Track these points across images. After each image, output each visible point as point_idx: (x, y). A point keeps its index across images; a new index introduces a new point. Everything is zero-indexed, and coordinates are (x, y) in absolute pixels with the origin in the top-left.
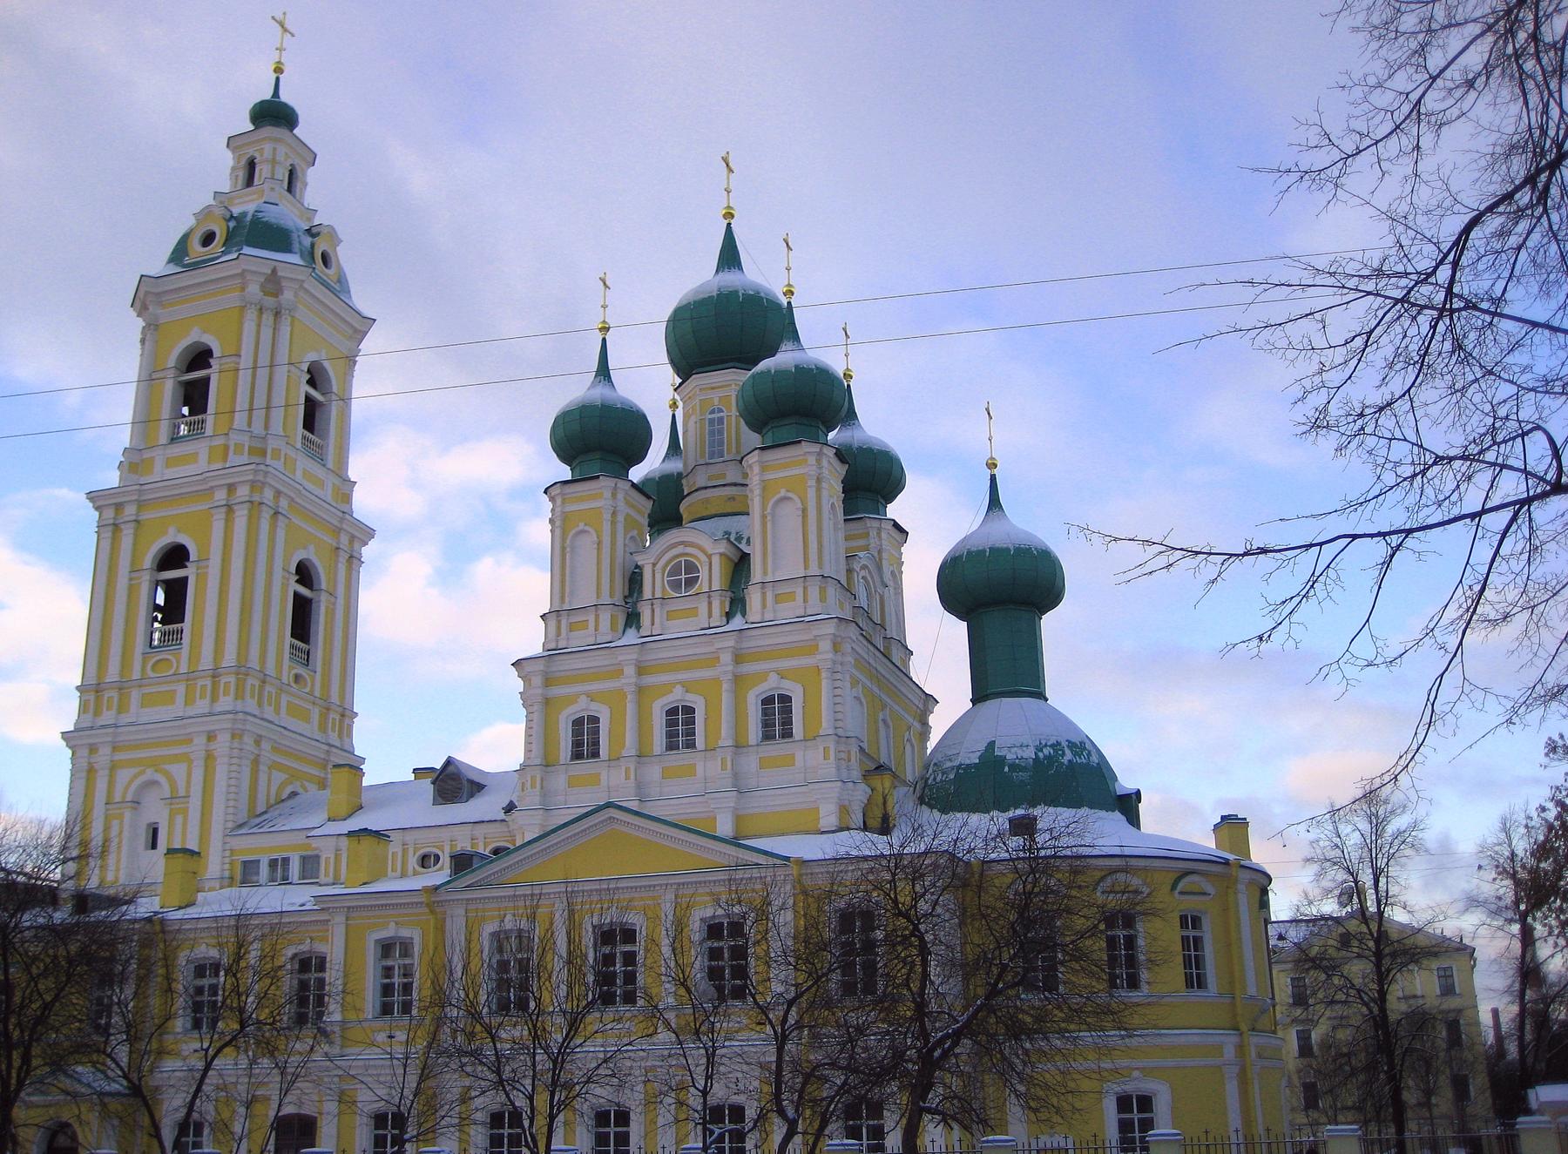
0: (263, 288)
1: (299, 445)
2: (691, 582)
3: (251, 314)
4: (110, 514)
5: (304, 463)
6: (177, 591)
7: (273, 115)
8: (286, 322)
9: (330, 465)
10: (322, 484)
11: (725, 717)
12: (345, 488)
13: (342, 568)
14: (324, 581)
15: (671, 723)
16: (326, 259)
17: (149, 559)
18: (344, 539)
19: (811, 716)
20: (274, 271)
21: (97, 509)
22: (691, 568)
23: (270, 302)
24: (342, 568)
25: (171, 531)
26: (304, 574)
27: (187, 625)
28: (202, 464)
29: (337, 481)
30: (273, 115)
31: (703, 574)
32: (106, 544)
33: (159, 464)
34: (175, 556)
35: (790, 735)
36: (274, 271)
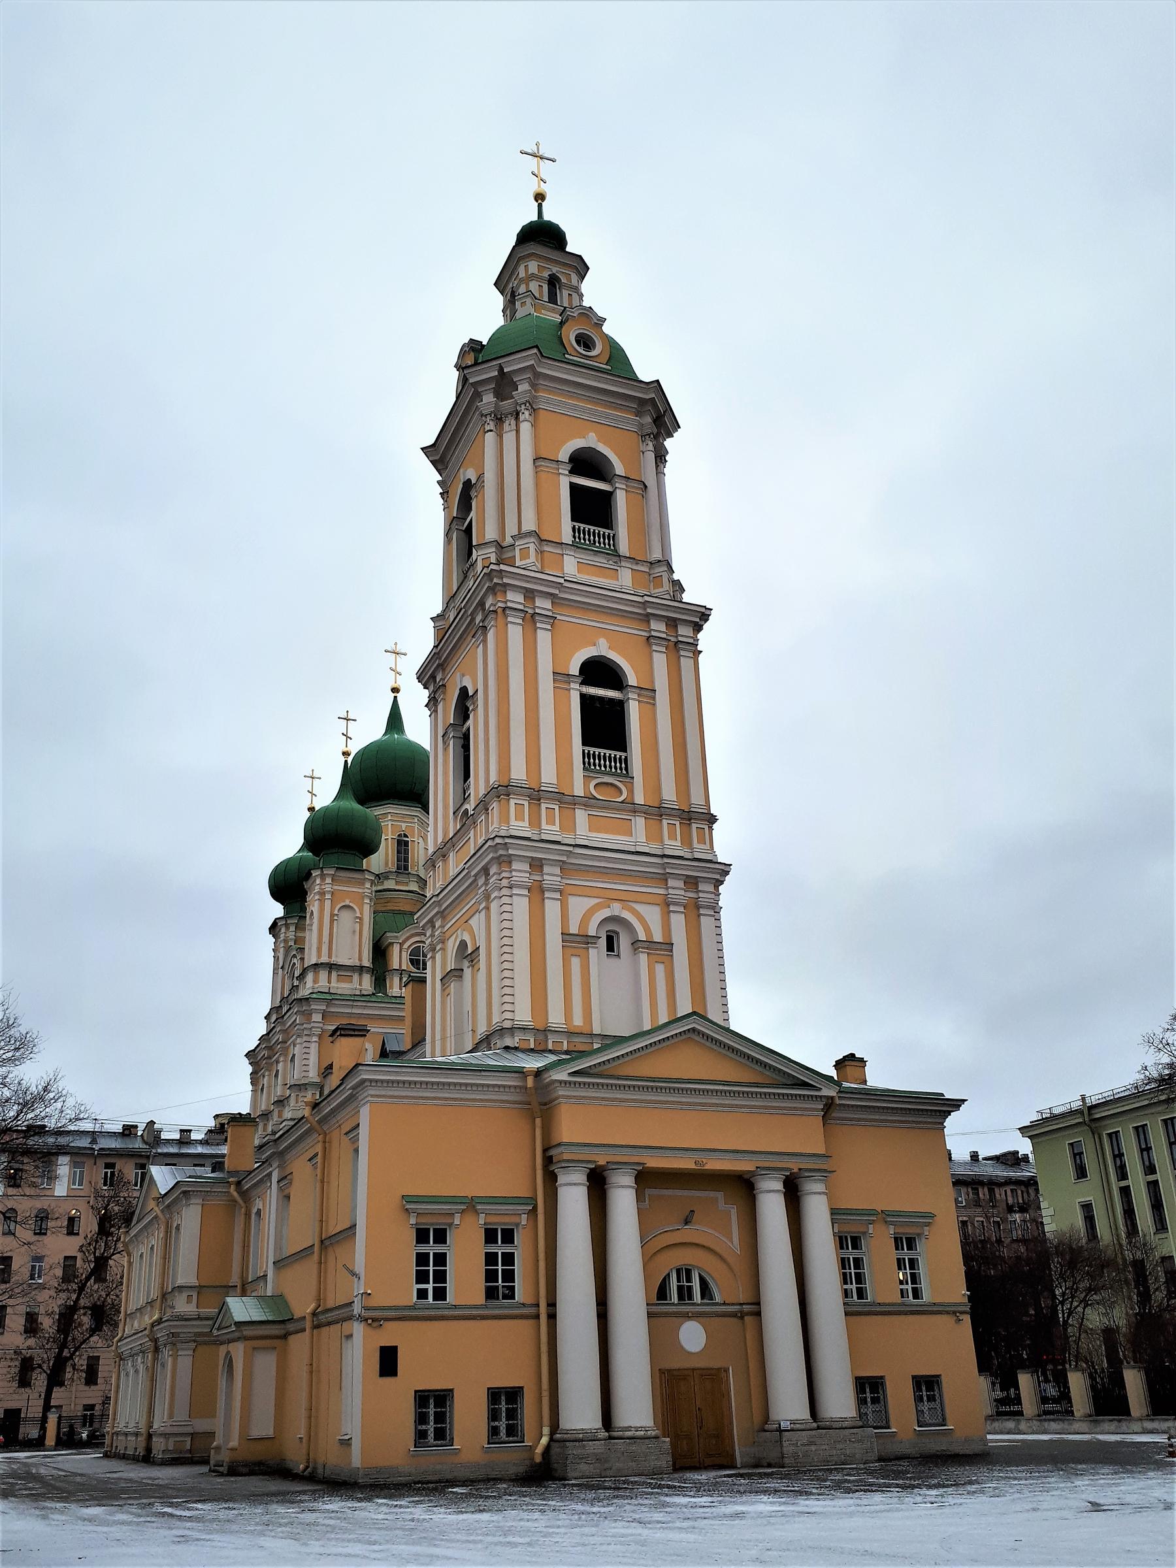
1: (567, 538)
3: (491, 426)
7: (541, 237)
8: (525, 415)
9: (624, 548)
13: (660, 660)
14: (632, 680)
16: (585, 342)
18: (659, 627)
20: (501, 369)
23: (507, 405)
30: (541, 237)
36: (501, 369)
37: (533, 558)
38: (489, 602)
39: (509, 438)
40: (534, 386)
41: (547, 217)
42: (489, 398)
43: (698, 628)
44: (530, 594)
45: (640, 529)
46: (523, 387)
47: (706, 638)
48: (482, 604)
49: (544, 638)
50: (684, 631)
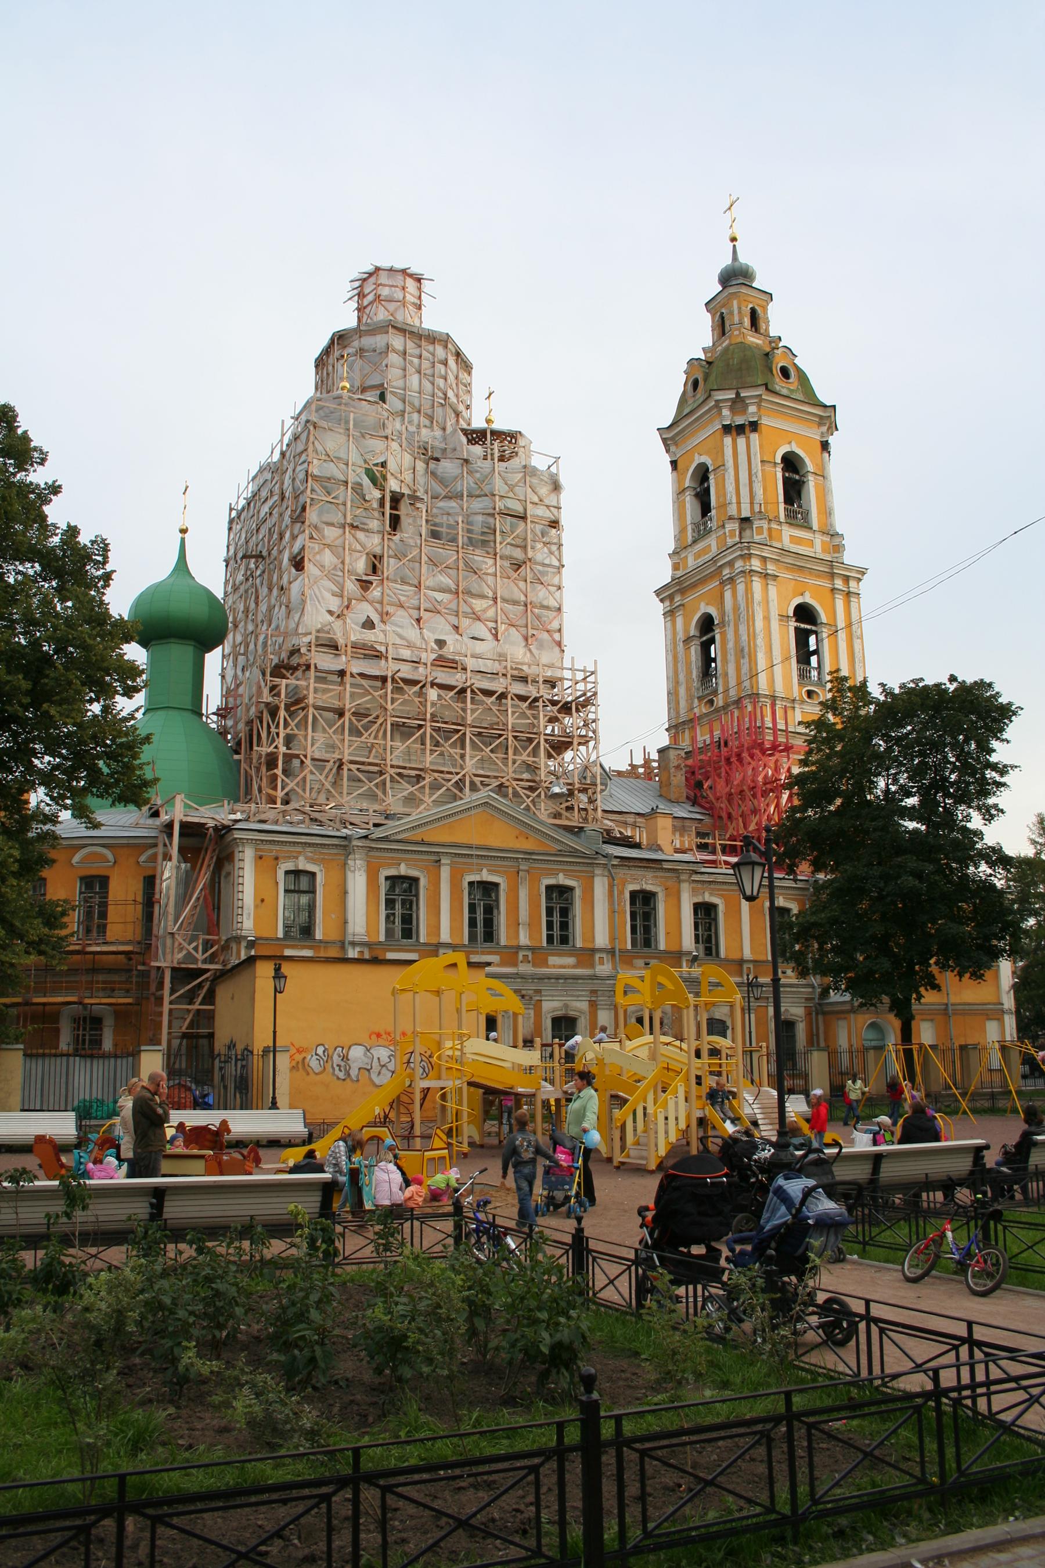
0: (732, 409)
1: (782, 518)
4: (667, 603)
5: (788, 533)
7: (735, 277)
9: (815, 527)
10: (811, 543)
12: (834, 540)
13: (840, 603)
14: (823, 618)
17: (693, 631)
18: (839, 583)
21: (662, 601)
24: (840, 603)
25: (702, 605)
26: (804, 613)
29: (827, 539)
30: (735, 277)
32: (669, 624)
37: (765, 534)
38: (739, 565)
40: (759, 406)
41: (743, 259)
43: (860, 580)
44: (764, 559)
45: (827, 512)
46: (752, 409)
47: (865, 588)
48: (731, 564)
49: (773, 591)
50: (853, 584)
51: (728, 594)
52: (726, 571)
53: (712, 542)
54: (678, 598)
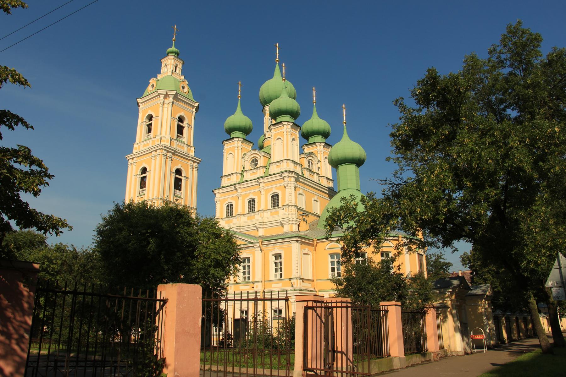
2: (256, 165)
3: (161, 105)
6: (143, 180)
11: (264, 202)
14: (184, 174)
15: (250, 205)
17: (139, 172)
19: (284, 200)
20: (167, 93)
22: (256, 161)
27: (146, 188)
28: (150, 145)
31: (259, 162)
33: (142, 146)
34: (144, 170)
35: (278, 206)
36: (167, 93)
39: (165, 109)
42: (162, 98)
48: (156, 151)
51: (153, 161)
52: (154, 153)
53: (150, 142)
54: (135, 159)
